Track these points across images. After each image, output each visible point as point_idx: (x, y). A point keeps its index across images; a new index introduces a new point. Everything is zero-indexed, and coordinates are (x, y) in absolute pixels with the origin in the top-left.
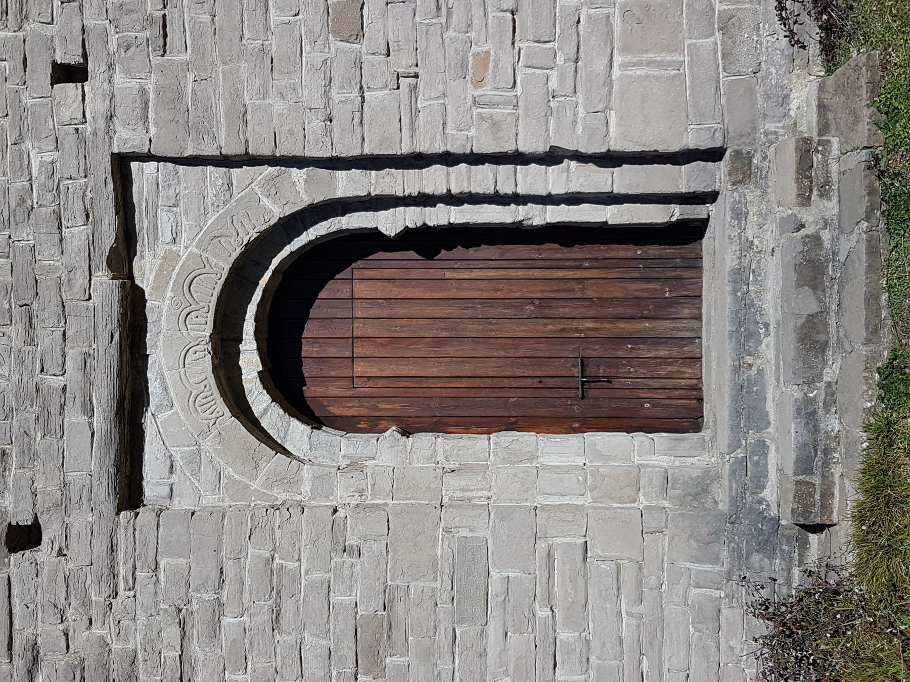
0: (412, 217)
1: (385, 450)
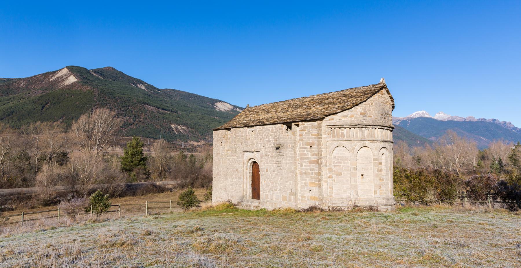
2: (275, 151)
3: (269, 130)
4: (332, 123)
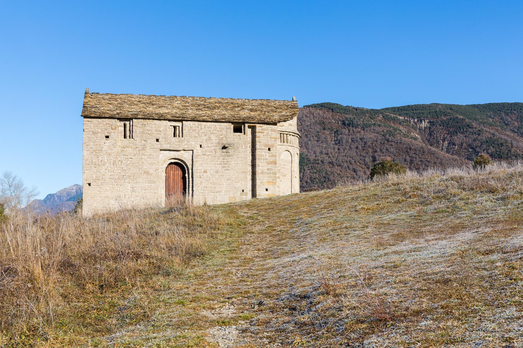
0: (187, 177)
1: (164, 175)
2: (219, 152)
3: (208, 127)
4: (283, 129)
